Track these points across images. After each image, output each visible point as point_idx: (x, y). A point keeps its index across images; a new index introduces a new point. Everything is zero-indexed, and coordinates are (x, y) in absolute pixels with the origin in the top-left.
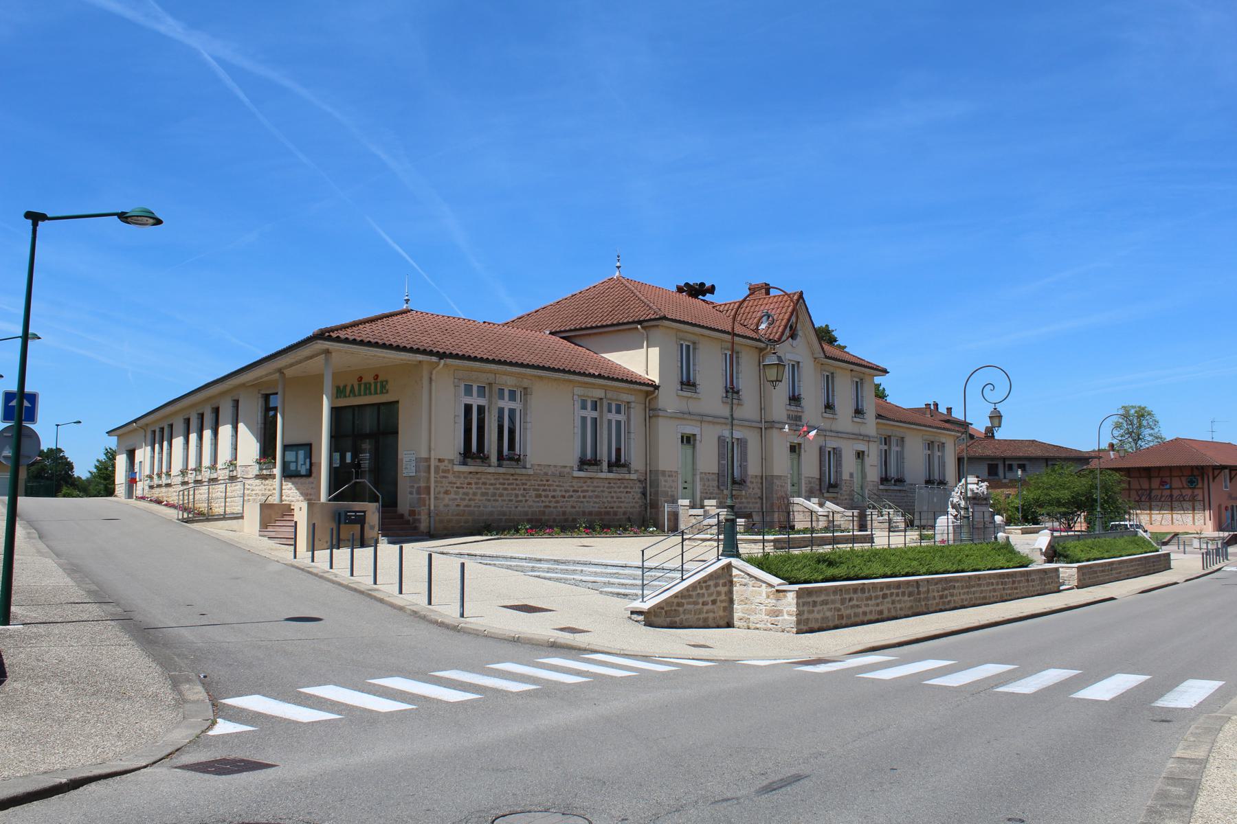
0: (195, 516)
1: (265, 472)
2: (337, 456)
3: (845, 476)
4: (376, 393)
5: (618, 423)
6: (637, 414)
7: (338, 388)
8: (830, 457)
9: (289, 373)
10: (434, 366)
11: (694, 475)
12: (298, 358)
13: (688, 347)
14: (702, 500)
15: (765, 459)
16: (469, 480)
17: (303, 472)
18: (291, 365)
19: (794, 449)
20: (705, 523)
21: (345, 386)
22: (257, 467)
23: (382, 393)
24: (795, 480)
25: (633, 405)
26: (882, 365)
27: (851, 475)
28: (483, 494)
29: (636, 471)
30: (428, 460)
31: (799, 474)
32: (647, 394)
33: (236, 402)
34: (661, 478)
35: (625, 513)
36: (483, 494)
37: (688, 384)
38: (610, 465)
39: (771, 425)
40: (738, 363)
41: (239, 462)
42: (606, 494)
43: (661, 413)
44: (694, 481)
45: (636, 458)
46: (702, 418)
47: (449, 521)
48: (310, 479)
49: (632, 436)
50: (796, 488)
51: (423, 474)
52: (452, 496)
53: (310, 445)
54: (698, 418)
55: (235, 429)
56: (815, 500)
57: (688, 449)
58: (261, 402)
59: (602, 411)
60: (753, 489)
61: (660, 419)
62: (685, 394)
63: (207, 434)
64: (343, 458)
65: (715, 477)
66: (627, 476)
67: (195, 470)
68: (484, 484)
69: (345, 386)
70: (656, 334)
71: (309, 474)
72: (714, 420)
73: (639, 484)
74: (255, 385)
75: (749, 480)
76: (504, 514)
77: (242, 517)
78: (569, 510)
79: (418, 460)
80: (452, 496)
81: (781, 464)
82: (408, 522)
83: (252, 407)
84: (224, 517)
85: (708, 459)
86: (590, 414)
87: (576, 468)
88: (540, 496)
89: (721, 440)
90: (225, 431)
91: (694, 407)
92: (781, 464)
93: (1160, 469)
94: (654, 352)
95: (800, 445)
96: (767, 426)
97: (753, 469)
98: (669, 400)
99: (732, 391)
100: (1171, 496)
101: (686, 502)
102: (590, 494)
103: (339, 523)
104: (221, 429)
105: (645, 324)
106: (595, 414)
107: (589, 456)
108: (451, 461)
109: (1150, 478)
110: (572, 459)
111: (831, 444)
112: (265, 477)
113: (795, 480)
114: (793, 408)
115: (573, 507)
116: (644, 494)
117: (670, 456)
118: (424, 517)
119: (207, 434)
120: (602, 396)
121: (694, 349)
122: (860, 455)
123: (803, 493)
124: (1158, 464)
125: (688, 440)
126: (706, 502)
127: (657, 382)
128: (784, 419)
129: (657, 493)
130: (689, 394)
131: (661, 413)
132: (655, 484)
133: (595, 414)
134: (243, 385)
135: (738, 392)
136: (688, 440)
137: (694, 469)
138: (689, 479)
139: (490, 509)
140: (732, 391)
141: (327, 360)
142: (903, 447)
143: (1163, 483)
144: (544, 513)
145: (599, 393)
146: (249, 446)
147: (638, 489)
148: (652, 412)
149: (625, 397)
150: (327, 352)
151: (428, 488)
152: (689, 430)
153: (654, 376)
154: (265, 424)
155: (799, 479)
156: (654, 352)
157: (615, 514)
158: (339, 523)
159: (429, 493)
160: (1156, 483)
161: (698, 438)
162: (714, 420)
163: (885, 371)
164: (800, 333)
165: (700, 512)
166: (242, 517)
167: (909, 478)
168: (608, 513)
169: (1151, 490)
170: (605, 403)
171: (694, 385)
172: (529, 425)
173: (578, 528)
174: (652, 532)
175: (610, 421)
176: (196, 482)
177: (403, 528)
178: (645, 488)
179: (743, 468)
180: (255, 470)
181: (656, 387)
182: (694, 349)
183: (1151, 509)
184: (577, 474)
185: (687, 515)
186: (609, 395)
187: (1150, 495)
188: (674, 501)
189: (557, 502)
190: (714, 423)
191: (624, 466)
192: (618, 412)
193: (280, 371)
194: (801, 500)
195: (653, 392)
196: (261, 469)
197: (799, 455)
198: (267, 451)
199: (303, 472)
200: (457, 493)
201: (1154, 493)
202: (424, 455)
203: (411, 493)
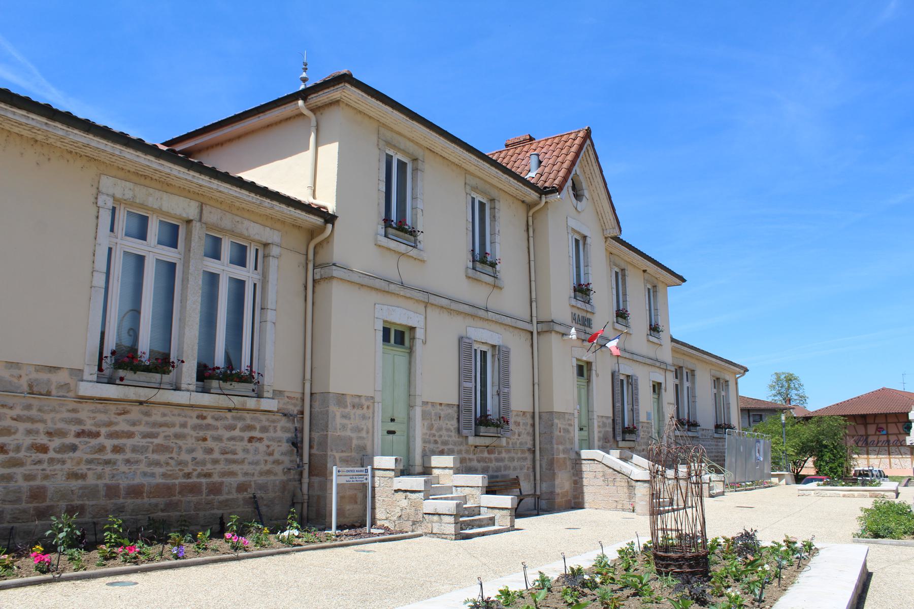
3: (643, 418)
5: (239, 285)
6: (283, 276)
8: (623, 386)
11: (411, 406)
13: (402, 166)
14: (426, 456)
15: (537, 385)
19: (583, 370)
20: (430, 505)
24: (584, 422)
25: (275, 251)
27: (648, 414)
29: (277, 394)
31: (589, 411)
32: (313, 233)
34: (335, 411)
35: (241, 488)
37: (398, 226)
38: (205, 374)
39: (548, 327)
40: (493, 218)
42: (190, 442)
43: (336, 272)
44: (409, 419)
45: (276, 360)
46: (428, 299)
49: (270, 315)
50: (584, 433)
54: (420, 296)
56: (615, 453)
57: (398, 355)
59: (188, 249)
60: (519, 435)
61: (335, 282)
62: (393, 245)
65: (453, 412)
66: (251, 403)
70: (334, 119)
72: (453, 306)
73: (283, 422)
75: (512, 421)
81: (564, 395)
85: (439, 378)
86: (154, 251)
87: (90, 371)
89: (464, 345)
91: (411, 273)
92: (564, 395)
93: (875, 416)
94: (330, 153)
95: (589, 364)
96: (541, 329)
97: (520, 401)
98: (358, 244)
99: (482, 260)
100: (888, 441)
101: (385, 462)
102: (137, 441)
106: (169, 254)
107: (145, 345)
109: (866, 425)
110: (80, 351)
111: (627, 369)
113: (584, 422)
114: (580, 304)
115: (74, 476)
116: (296, 444)
117: (355, 365)
121: (415, 170)
122: (657, 388)
123: (596, 443)
124: (875, 411)
125: (398, 337)
126: (436, 461)
127: (331, 207)
128: (568, 320)
129: (323, 444)
130: (402, 248)
131: (336, 272)
132: (319, 421)
133: (169, 254)
135: (493, 265)
136: (398, 337)
137: (410, 395)
138: (400, 415)
140: (482, 260)
142: (693, 383)
143: (879, 429)
147: (282, 431)
148: (318, 272)
149: (256, 231)
152: (401, 316)
153: (327, 200)
155: (590, 419)
156: (330, 153)
157: (215, 489)
160: (872, 429)
161: (419, 334)
162: (453, 306)
164: (586, 193)
165: (416, 482)
167: (700, 420)
168: (194, 489)
169: (867, 436)
170: (198, 231)
171: (413, 233)
174: (289, 542)
175: (212, 279)
178: (299, 431)
179: (503, 396)
181: (330, 219)
182: (415, 170)
183: (868, 454)
184: (89, 389)
185: (392, 493)
186: (212, 216)
187: (866, 440)
188: (364, 459)
190: (450, 311)
191: (247, 379)
192: (240, 260)
194: (598, 454)
195: (322, 230)
201: (870, 439)
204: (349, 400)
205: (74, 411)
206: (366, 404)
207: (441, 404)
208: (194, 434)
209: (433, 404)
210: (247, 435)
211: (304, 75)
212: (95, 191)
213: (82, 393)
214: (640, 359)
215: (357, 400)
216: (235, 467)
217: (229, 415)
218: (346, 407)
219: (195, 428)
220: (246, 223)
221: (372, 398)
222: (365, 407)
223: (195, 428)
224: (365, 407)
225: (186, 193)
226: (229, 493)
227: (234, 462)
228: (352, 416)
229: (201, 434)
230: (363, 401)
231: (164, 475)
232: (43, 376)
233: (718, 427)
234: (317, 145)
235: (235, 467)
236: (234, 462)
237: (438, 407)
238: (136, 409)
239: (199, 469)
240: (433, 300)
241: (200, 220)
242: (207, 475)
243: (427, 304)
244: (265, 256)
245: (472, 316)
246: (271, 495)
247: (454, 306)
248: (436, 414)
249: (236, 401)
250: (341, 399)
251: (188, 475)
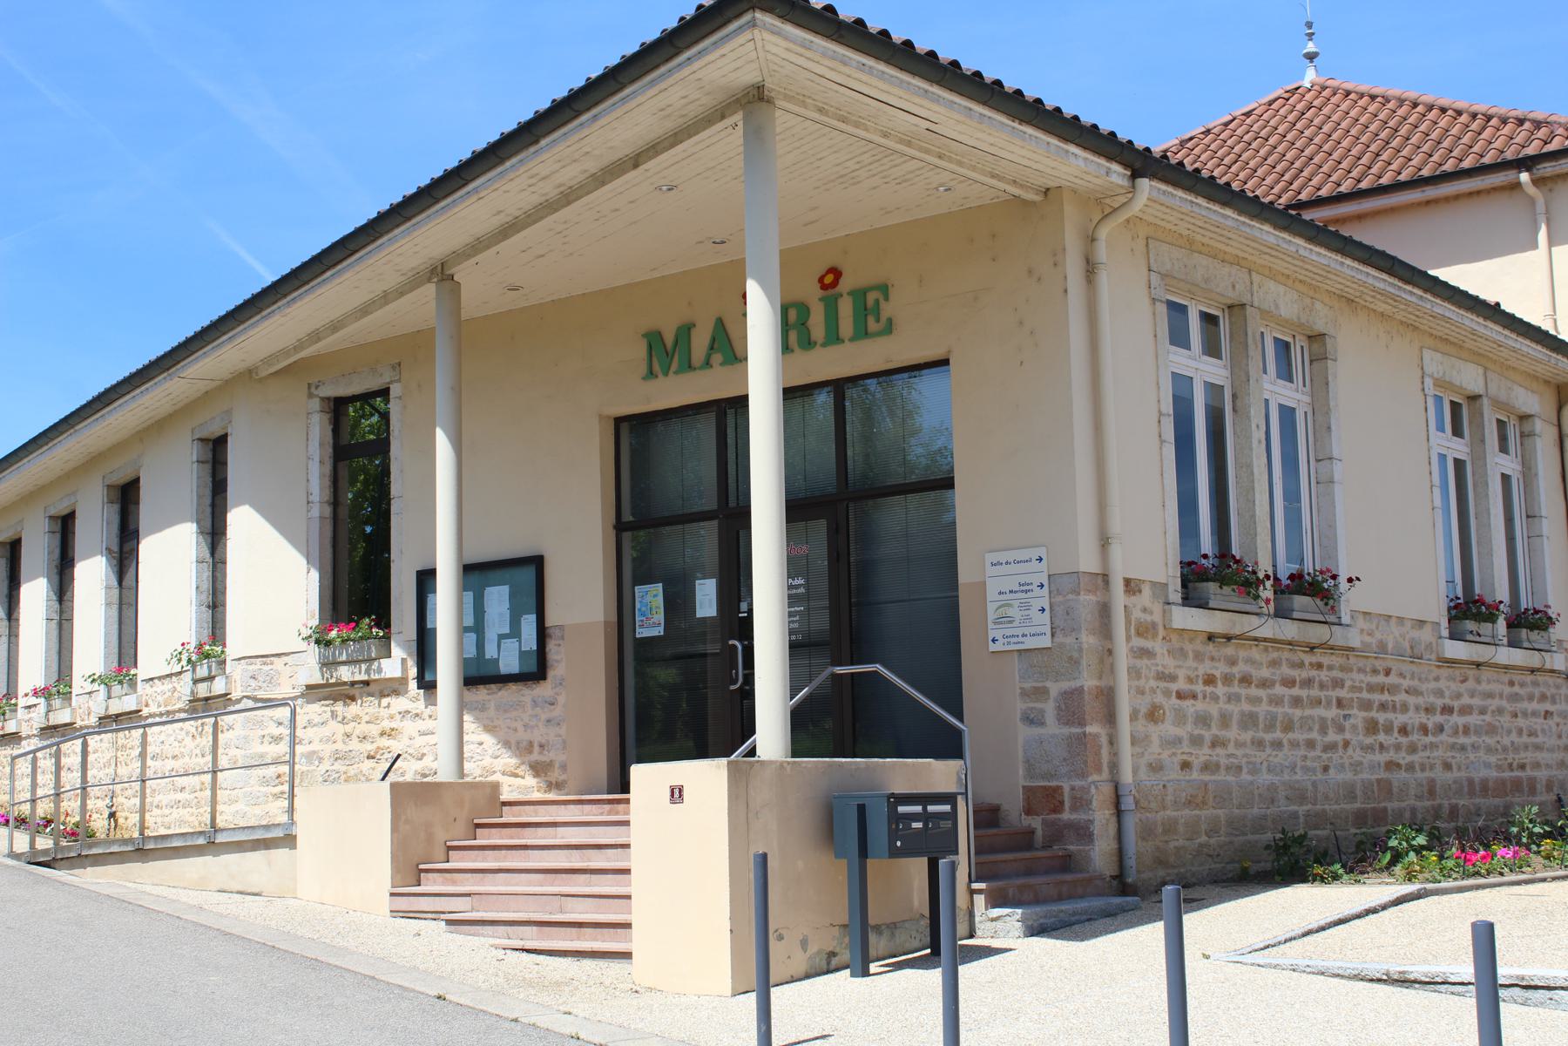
0: (70, 846)
1: (345, 674)
2: (651, 598)
4: (834, 338)
7: (654, 340)
9: (481, 286)
10: (1102, 207)
12: (571, 175)
16: (1205, 668)
17: (509, 662)
18: (477, 246)
21: (685, 331)
22: (313, 653)
23: (862, 333)
28: (1249, 720)
30: (1105, 578)
33: (216, 450)
36: (1249, 720)
41: (237, 641)
47: (1170, 827)
48: (543, 690)
51: (1089, 640)
52: (1169, 729)
53: (537, 562)
55: (215, 534)
58: (318, 429)
63: (92, 573)
64: (678, 602)
67: (44, 693)
68: (1246, 680)
69: (685, 331)
71: (536, 670)
74: (294, 370)
76: (1302, 797)
77: (289, 841)
78: (1440, 775)
79: (1061, 584)
80: (1169, 729)
82: (1024, 840)
83: (286, 453)
84: (209, 842)
88: (1372, 727)
90: (170, 551)
103: (863, 852)
104: (151, 548)
105: (1547, 169)
112: (345, 693)
118: (1101, 817)
119: (92, 573)
120: (1476, 386)
134: (247, 377)
139: (1265, 778)
141: (757, 137)
144: (1385, 787)
145: (1470, 378)
146: (276, 577)
150: (755, 99)
151: (1108, 698)
154: (335, 503)
158: (863, 852)
159: (1111, 718)
166: (289, 841)
172: (1338, 470)
173: (1143, 839)
176: (49, 730)
177: (1070, 873)
180: (308, 667)
189: (1413, 749)
193: (441, 274)
196: (328, 664)
198: (360, 585)
199: (509, 662)
200: (1180, 718)
202: (1088, 562)
203: (1032, 720)
205: (1437, 679)
211: (1311, 47)
212: (1420, 373)
213: (1449, 655)
217: (1529, 678)
225: (1477, 357)
231: (1499, 768)
232: (1415, 634)
234: (1551, 243)
238: (1471, 673)
242: (1522, 767)
244: (1522, 435)
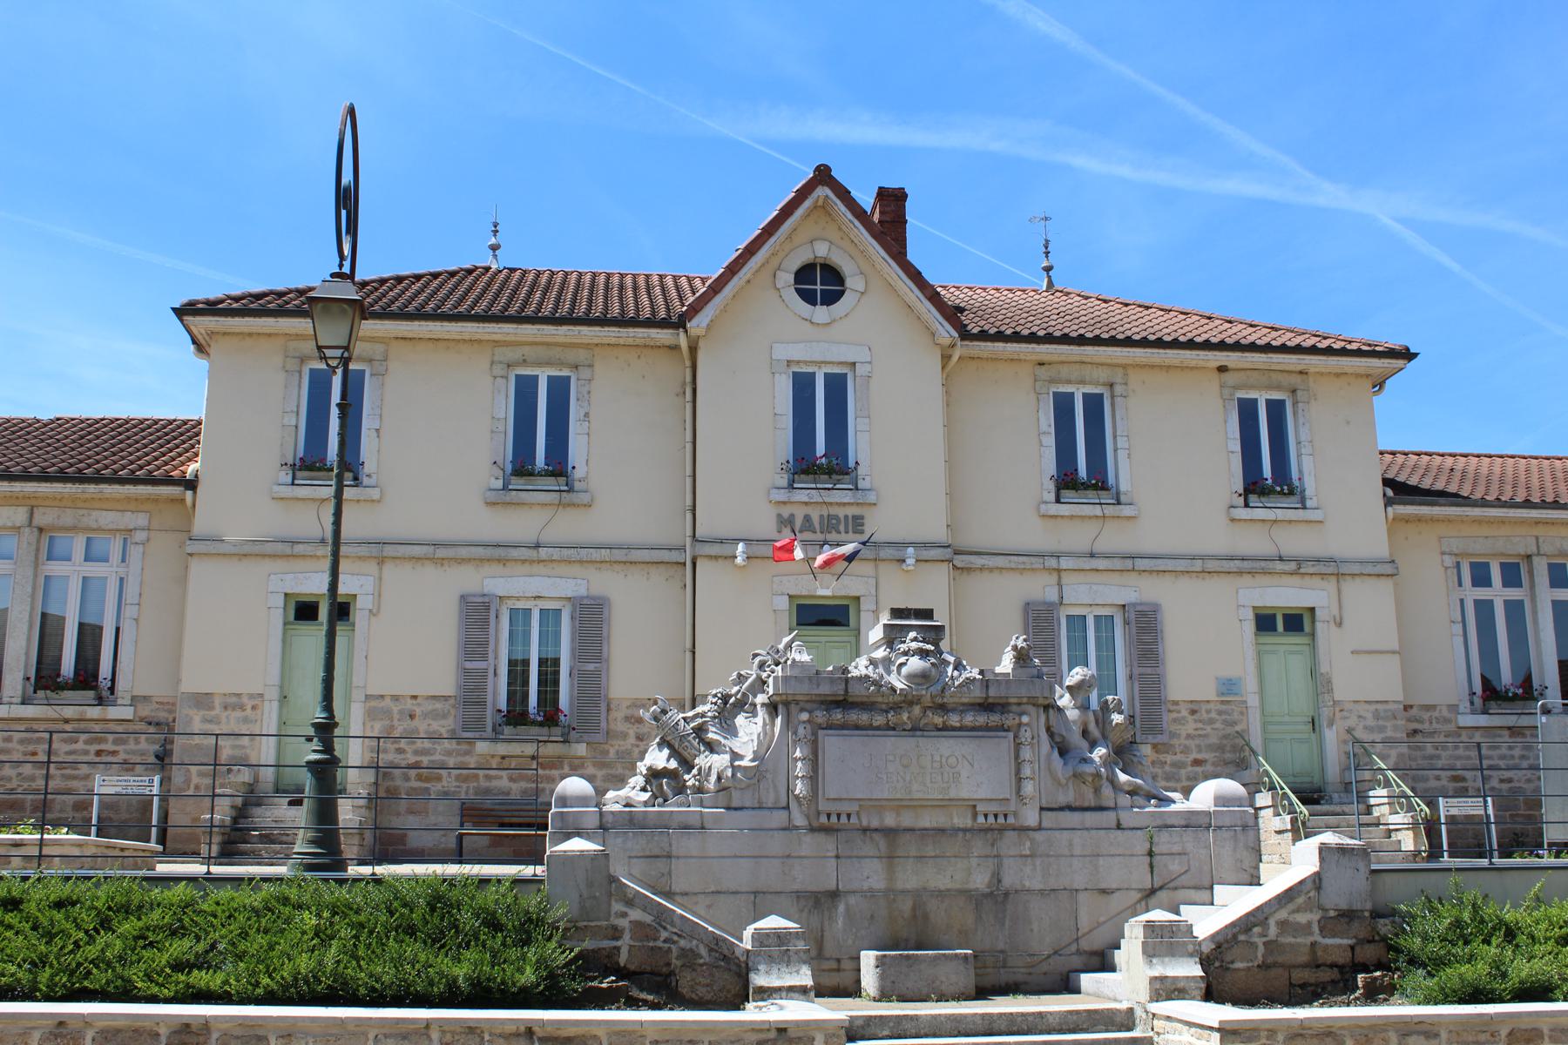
26: (1395, 342)
54: (374, 550)
66: (94, 712)
108: (1453, 708)
163: (1407, 355)
190: (441, 561)
197: (1313, 635)
204: (217, 702)
206: (249, 704)
207: (415, 697)
208: (21, 748)
209: (396, 698)
210: (94, 748)
214: (1181, 565)
215: (234, 700)
216: (75, 784)
218: (212, 708)
219: (21, 742)
220: (95, 513)
221: (261, 695)
222: (249, 707)
223: (21, 742)
224: (249, 707)
226: (61, 811)
227: (75, 778)
228: (224, 720)
229: (31, 748)
230: (245, 700)
233: (1492, 694)
235: (75, 784)
236: (75, 778)
237: (409, 701)
239: (26, 785)
240: (389, 551)
241: (30, 525)
243: (381, 561)
245: (499, 561)
246: (124, 816)
247: (441, 553)
248: (401, 712)
249: (69, 712)
250: (202, 700)
251: (12, 791)
